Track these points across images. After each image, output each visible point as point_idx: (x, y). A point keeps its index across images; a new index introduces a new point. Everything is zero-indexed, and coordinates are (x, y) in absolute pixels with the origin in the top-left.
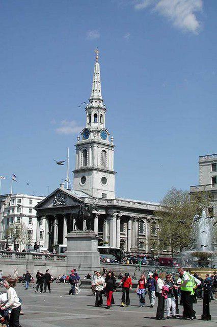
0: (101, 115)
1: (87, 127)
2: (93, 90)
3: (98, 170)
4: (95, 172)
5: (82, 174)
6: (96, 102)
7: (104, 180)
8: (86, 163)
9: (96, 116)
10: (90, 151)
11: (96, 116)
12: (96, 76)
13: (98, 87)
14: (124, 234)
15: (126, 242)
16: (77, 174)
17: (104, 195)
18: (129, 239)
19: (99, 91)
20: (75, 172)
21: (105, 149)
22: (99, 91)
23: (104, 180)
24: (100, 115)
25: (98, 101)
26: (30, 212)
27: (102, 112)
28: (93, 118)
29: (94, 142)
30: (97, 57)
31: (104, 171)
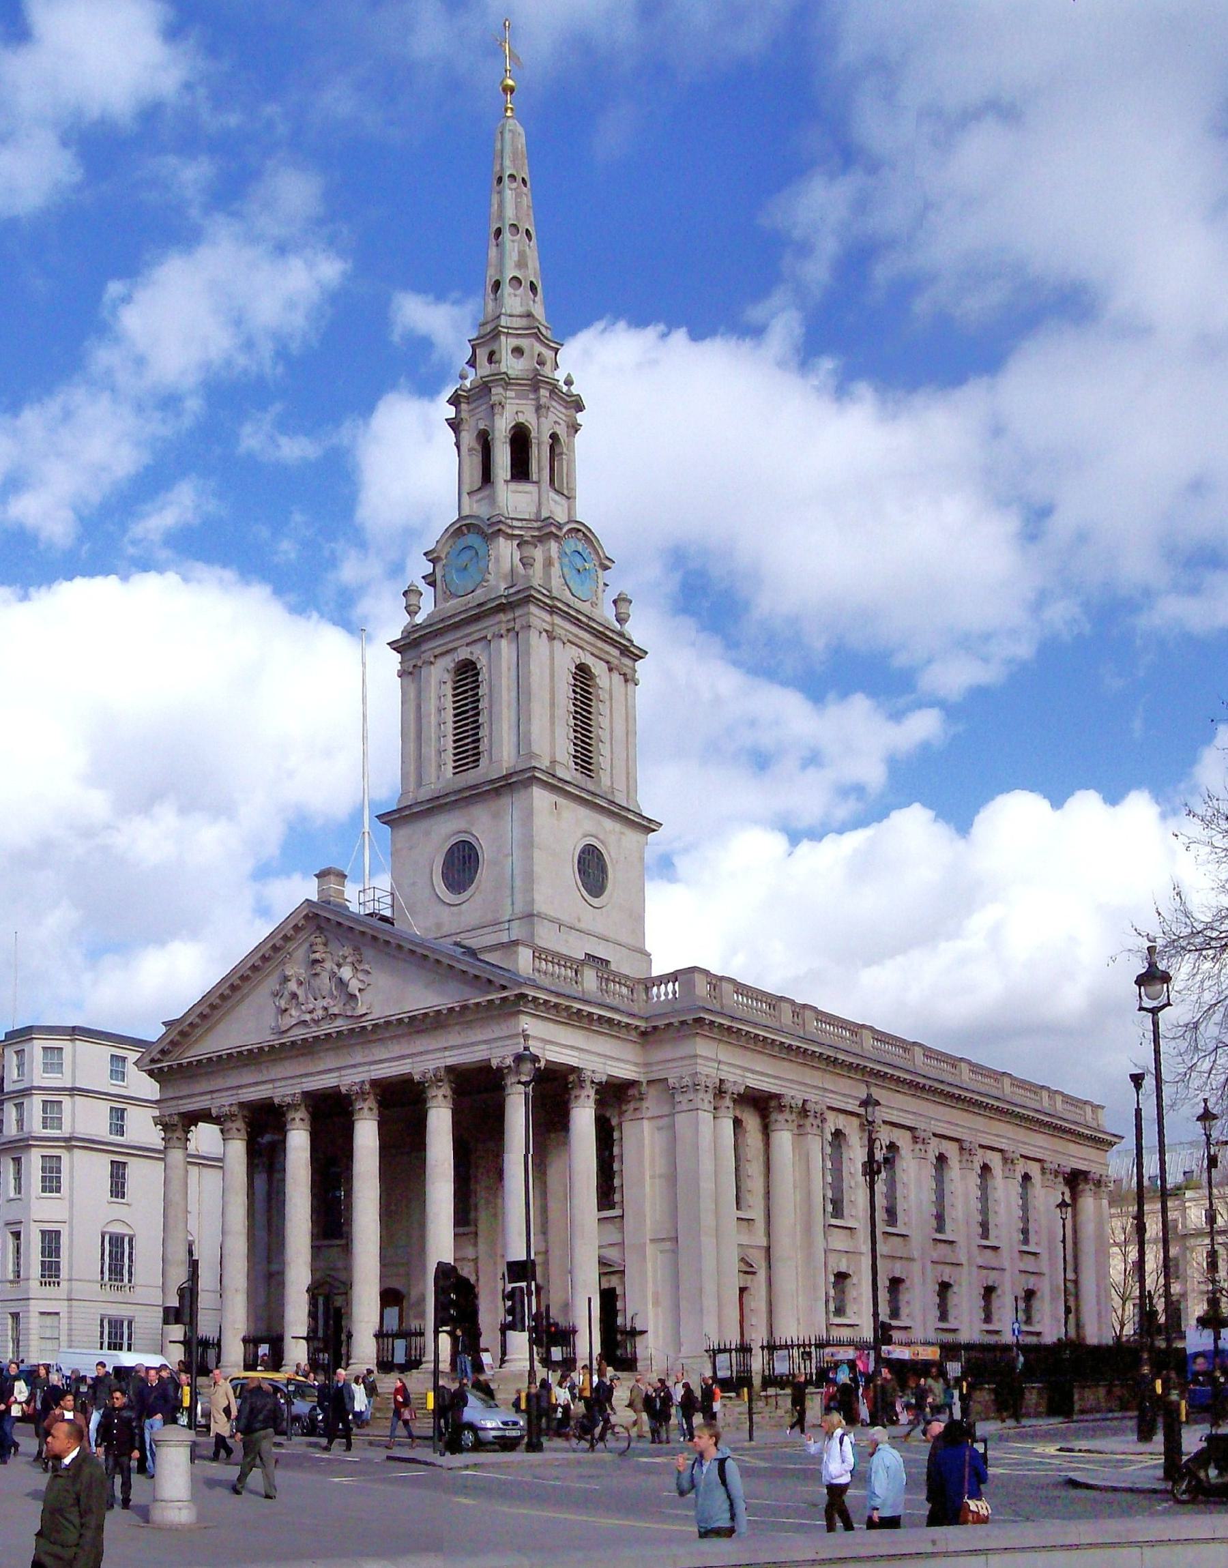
3: (557, 787)
4: (540, 797)
6: (518, 351)
9: (520, 440)
11: (520, 440)
12: (509, 195)
13: (522, 264)
18: (777, 1253)
24: (546, 440)
26: (118, 1075)
28: (502, 457)
30: (510, 82)
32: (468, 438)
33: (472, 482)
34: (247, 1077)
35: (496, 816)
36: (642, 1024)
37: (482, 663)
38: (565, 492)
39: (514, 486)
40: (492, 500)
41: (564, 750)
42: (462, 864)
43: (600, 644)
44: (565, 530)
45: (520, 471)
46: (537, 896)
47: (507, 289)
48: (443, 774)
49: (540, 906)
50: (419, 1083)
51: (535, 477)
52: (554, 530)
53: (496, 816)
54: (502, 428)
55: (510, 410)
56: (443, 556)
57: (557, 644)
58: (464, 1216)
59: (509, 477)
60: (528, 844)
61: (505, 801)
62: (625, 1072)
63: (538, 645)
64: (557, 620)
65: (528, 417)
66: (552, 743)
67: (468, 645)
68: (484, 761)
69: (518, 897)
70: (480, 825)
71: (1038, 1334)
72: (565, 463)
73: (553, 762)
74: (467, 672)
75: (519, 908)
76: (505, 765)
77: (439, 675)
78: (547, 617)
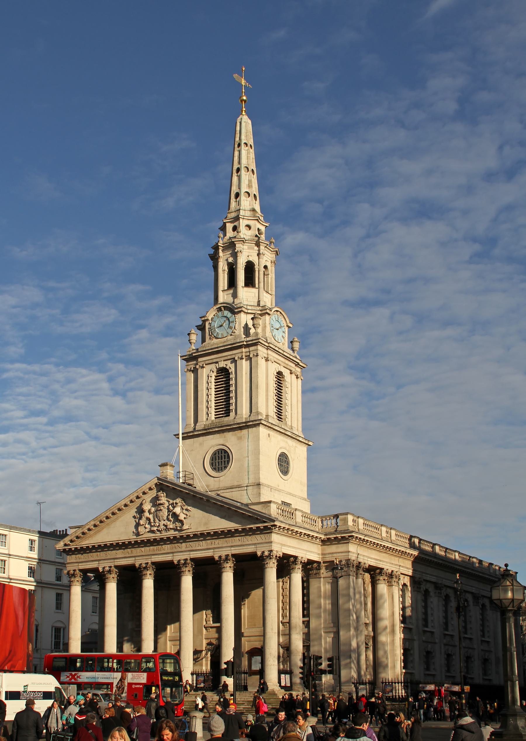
5: (213, 443)
7: (283, 463)
9: (250, 268)
11: (250, 268)
21: (283, 370)
23: (283, 463)
32: (223, 266)
33: (224, 287)
34: (120, 553)
35: (240, 438)
36: (323, 537)
37: (233, 370)
38: (270, 292)
39: (246, 289)
40: (235, 296)
41: (272, 411)
43: (287, 362)
44: (273, 310)
45: (250, 282)
46: (261, 476)
49: (262, 481)
50: (218, 561)
51: (257, 286)
52: (268, 311)
53: (240, 438)
56: (210, 319)
57: (269, 362)
58: (159, 629)
59: (244, 286)
60: (257, 452)
61: (245, 432)
62: (315, 557)
64: (270, 352)
65: (254, 259)
67: (224, 361)
68: (232, 414)
69: (251, 477)
71: (490, 680)
72: (270, 279)
73: (267, 416)
74: (224, 372)
75: (252, 481)
76: (244, 416)
77: (208, 375)
78: (265, 351)
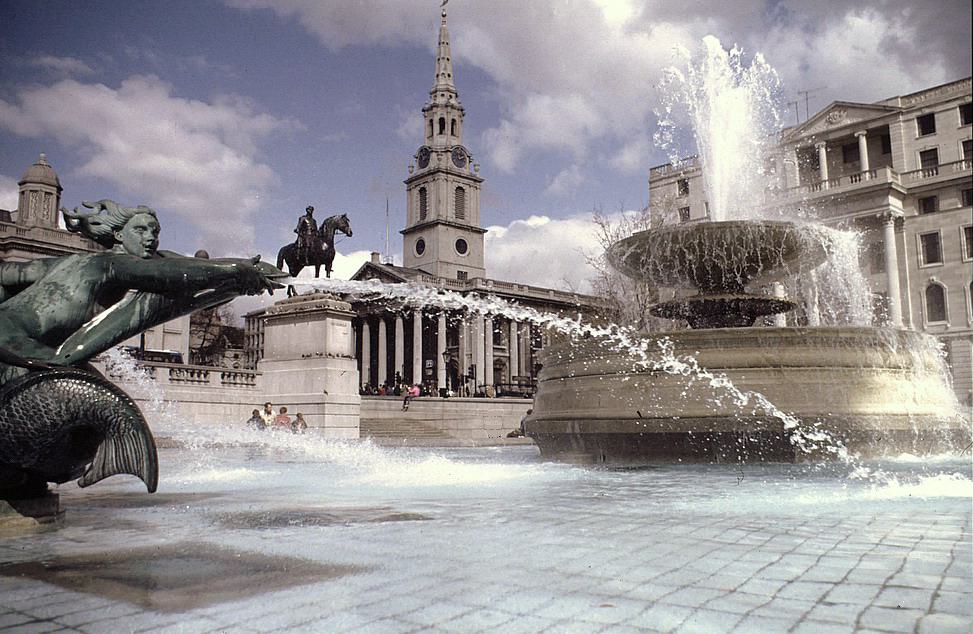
0: (454, 121)
1: (427, 144)
2: (438, 76)
3: (448, 224)
5: (416, 238)
6: (443, 95)
8: (424, 214)
9: (442, 121)
10: (431, 188)
11: (442, 121)
13: (445, 69)
14: (503, 350)
15: (507, 364)
16: (408, 237)
17: (462, 275)
19: (449, 75)
20: (405, 233)
21: (462, 185)
22: (449, 75)
24: (450, 122)
25: (447, 94)
27: (455, 114)
28: (437, 127)
29: (438, 171)
31: (461, 227)
42: (421, 246)
47: (440, 77)
48: (416, 220)
54: (436, 119)
55: (439, 113)
63: (443, 184)
66: (448, 212)
70: (425, 236)
77: (416, 192)
